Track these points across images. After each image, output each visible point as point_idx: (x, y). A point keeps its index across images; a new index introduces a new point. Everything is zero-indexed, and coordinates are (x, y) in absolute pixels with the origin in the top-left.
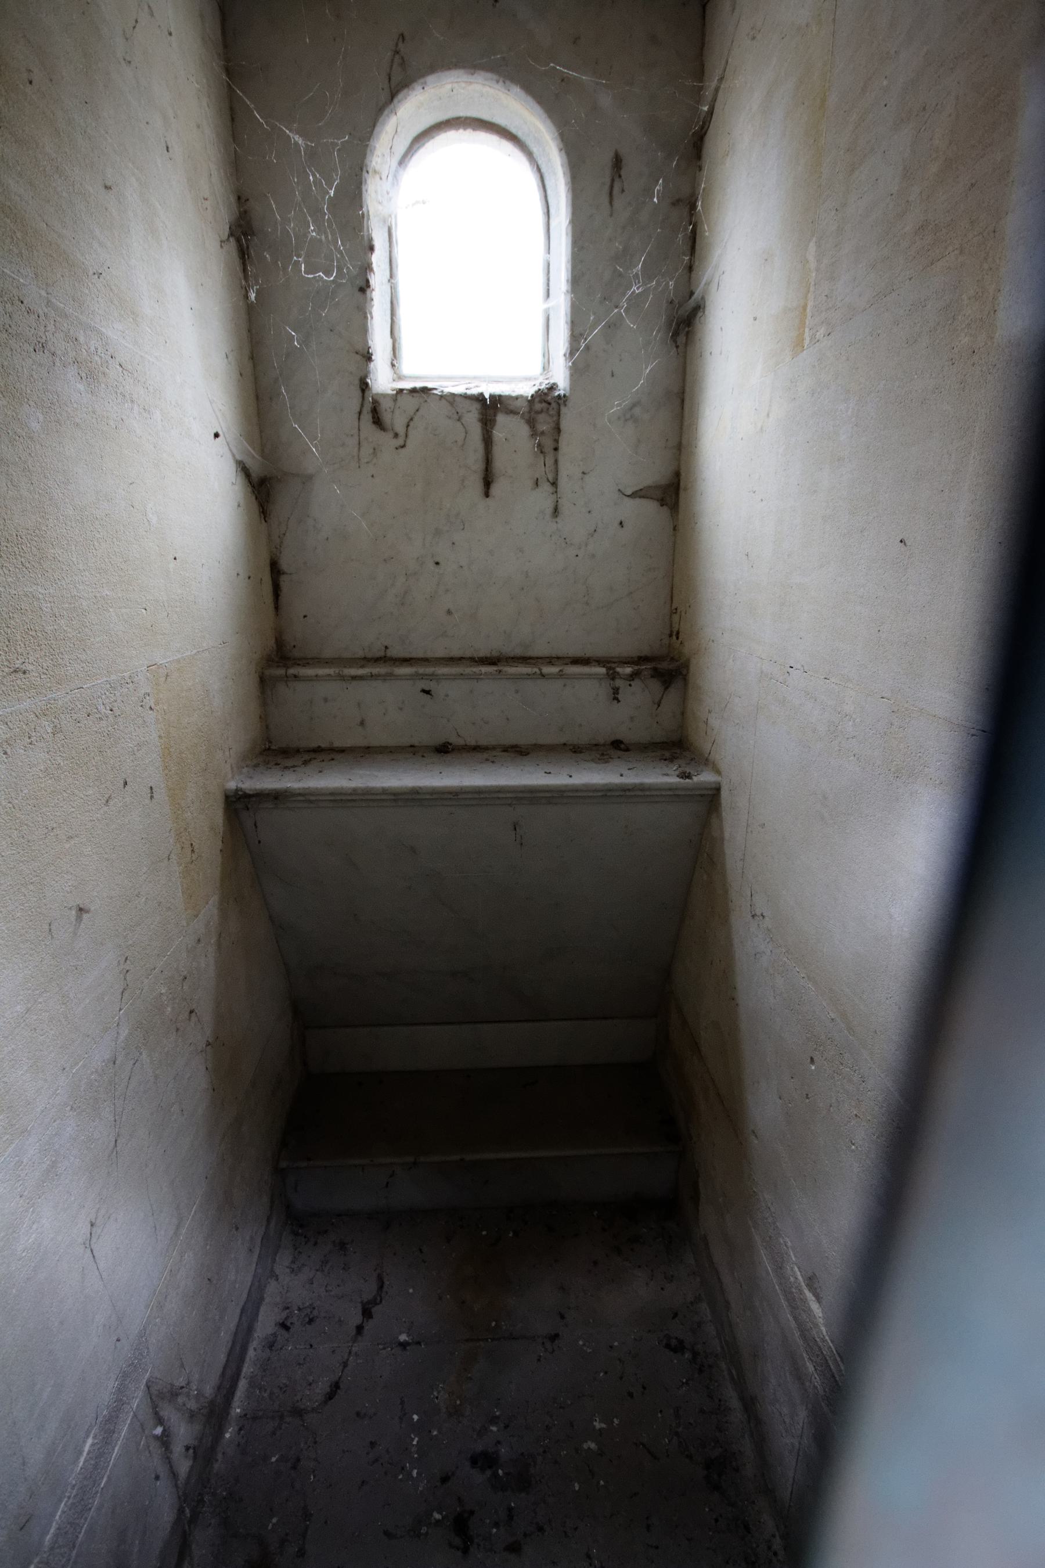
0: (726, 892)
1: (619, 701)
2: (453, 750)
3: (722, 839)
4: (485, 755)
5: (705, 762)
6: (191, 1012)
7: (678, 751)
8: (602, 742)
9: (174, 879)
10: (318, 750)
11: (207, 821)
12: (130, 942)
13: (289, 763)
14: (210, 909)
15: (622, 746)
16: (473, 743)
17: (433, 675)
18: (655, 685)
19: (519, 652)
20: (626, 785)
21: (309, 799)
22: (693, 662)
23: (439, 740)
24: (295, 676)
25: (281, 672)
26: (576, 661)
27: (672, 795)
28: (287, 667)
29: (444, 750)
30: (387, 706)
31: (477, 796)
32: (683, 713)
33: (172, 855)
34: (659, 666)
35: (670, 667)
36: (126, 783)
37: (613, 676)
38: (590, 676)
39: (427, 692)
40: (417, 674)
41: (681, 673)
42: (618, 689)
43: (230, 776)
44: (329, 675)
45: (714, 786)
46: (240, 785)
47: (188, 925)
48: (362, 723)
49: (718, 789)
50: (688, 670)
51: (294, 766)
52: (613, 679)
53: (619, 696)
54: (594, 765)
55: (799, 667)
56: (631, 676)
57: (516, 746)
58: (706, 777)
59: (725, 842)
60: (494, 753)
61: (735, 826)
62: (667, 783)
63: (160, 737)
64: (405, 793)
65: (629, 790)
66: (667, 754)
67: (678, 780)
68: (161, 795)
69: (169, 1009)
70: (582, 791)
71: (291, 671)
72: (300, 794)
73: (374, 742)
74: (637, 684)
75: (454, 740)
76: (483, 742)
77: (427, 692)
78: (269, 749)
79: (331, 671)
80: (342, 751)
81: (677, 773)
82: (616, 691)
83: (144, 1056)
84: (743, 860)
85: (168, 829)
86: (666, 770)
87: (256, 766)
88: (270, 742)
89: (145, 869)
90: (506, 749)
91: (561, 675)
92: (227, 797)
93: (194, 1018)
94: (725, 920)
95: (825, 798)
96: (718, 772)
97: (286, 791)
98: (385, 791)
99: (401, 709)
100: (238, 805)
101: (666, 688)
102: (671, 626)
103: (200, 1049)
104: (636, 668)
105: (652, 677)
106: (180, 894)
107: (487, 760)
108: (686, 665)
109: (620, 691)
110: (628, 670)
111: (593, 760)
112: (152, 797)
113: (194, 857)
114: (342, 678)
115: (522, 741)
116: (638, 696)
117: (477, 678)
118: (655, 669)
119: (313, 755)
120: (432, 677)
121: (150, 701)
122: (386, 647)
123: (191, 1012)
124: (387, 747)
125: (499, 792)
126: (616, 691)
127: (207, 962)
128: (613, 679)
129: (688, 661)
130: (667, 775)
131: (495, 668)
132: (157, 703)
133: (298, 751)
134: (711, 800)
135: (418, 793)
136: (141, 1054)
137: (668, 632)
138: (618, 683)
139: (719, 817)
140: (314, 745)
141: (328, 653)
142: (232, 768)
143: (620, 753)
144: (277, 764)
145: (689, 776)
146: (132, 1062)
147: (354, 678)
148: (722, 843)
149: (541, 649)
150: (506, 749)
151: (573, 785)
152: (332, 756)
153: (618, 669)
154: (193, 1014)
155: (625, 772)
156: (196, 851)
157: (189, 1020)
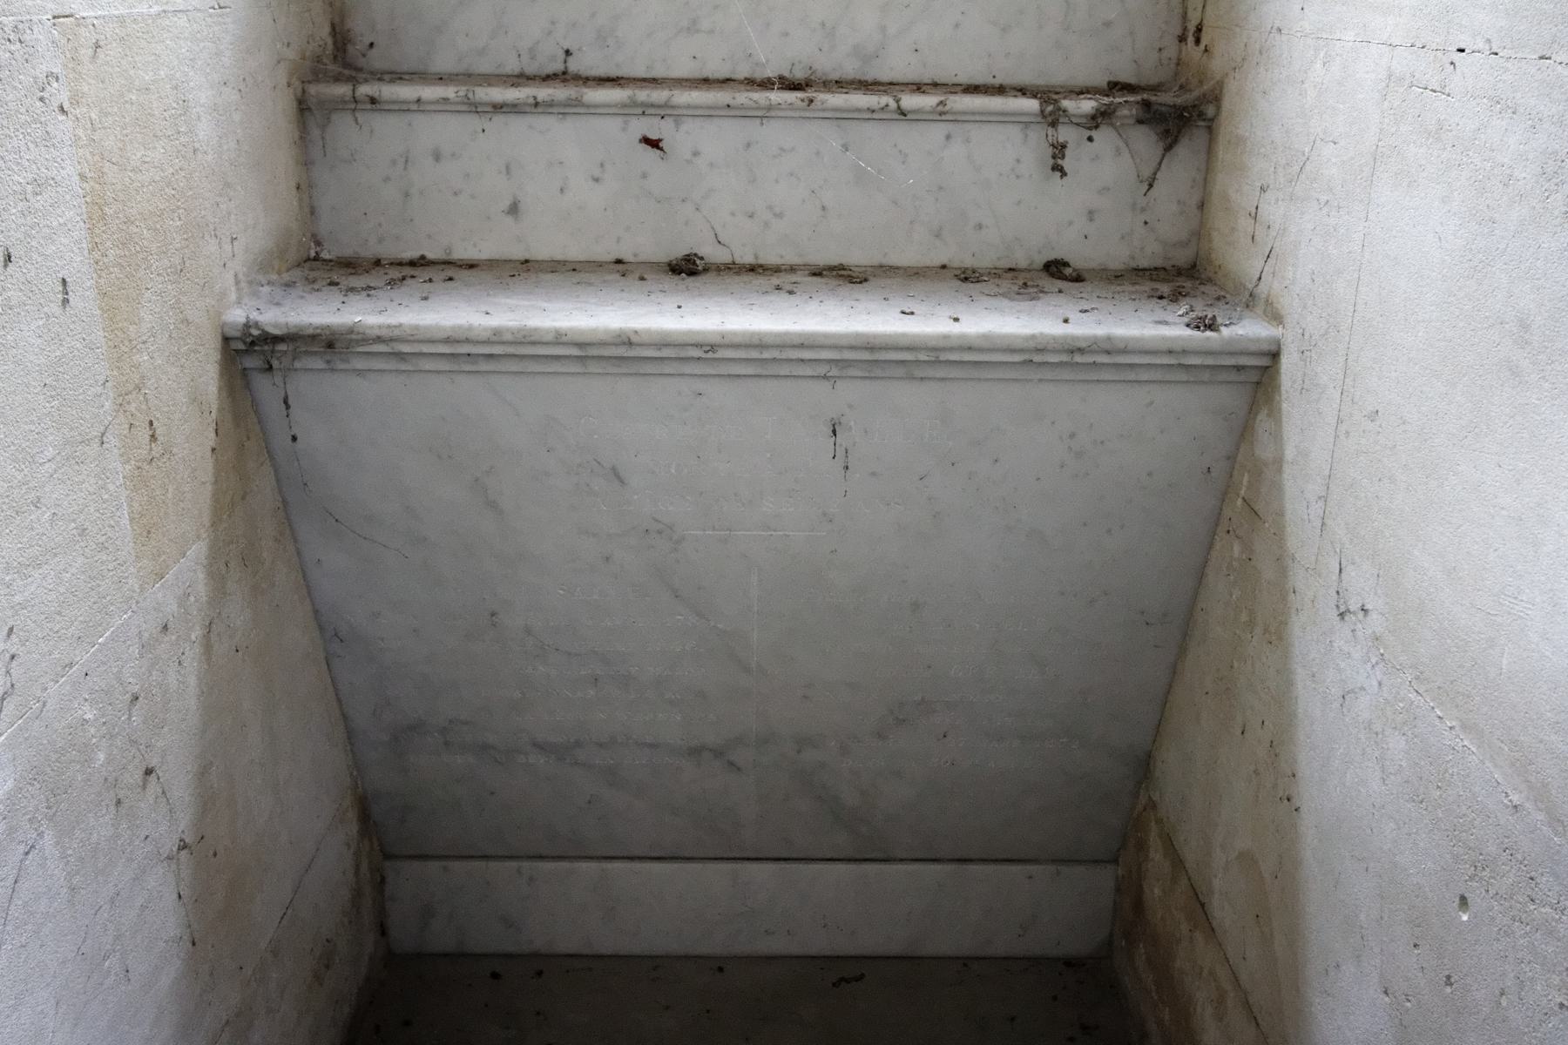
0: (1283, 571)
1: (1064, 174)
2: (706, 270)
3: (1279, 462)
4: (775, 281)
5: (1250, 300)
6: (149, 772)
7: (1188, 284)
8: (1023, 264)
9: (111, 487)
10: (421, 263)
11: (188, 384)
12: (18, 598)
13: (356, 282)
14: (190, 566)
15: (1068, 271)
16: (749, 259)
17: (666, 105)
18: (1145, 141)
19: (850, 69)
20: (1075, 338)
21: (397, 351)
22: (1231, 87)
23: (679, 251)
24: (373, 101)
25: (342, 90)
26: (973, 89)
27: (1174, 365)
28: (354, 81)
29: (686, 268)
30: (566, 173)
31: (754, 354)
32: (1202, 206)
33: (109, 437)
34: (1153, 98)
35: (1179, 101)
36: (8, 258)
37: (1053, 118)
38: (1004, 118)
39: (654, 144)
40: (633, 104)
41: (1201, 115)
42: (1064, 146)
43: (233, 297)
44: (446, 100)
45: (1265, 347)
46: (255, 316)
47: (142, 589)
48: (514, 209)
49: (1275, 355)
50: (1219, 108)
51: (369, 288)
52: (1054, 124)
53: (1066, 164)
54: (1006, 302)
55: (1481, 45)
56: (1093, 117)
57: (842, 267)
58: (1248, 330)
59: (1288, 471)
60: (794, 278)
61: (1312, 436)
62: (1164, 338)
63: (83, 177)
64: (603, 344)
65: (1081, 351)
66: (1165, 289)
67: (1189, 332)
68: (84, 299)
69: (102, 756)
70: (980, 350)
71: (365, 90)
72: (379, 339)
73: (541, 252)
74: (1105, 137)
75: (710, 252)
76: (770, 258)
77: (654, 144)
78: (316, 259)
79: (449, 92)
80: (472, 266)
81: (1186, 320)
82: (1059, 149)
83: (49, 839)
84: (1324, 499)
85: (102, 379)
86: (1160, 315)
87: (289, 285)
88: (318, 243)
89: (50, 452)
90: (817, 273)
91: (941, 114)
92: (226, 340)
93: (153, 787)
94: (1277, 634)
95: (1524, 326)
96: (1276, 318)
97: (351, 330)
98: (559, 338)
99: (597, 180)
100: (250, 356)
101: (1168, 148)
102: (1184, 16)
103: (165, 852)
104: (1106, 100)
105: (1140, 122)
106: (125, 521)
107: (778, 288)
108: (1216, 97)
109: (1068, 152)
110: (1087, 105)
111: (1004, 295)
112: (65, 302)
113: (157, 449)
114: (474, 108)
115: (856, 257)
116: (1108, 162)
117: (765, 114)
118: (1146, 104)
119: (408, 271)
120: (663, 111)
121: (60, 93)
122: (568, 53)
123: (149, 772)
124: (565, 263)
125: (802, 346)
126: (1059, 149)
127: (183, 678)
128: (1054, 124)
129: (1220, 85)
130: (1166, 323)
131: (800, 94)
132: (76, 100)
133: (378, 263)
134: (1260, 376)
135: (630, 344)
136: (41, 835)
137: (1179, 32)
138: (1065, 133)
139: (1275, 414)
140: (411, 254)
141: (443, 62)
142: (237, 283)
143: (1060, 284)
144: (332, 284)
145: (1212, 326)
146: (22, 848)
147: (498, 108)
148: (1280, 470)
149: (896, 66)
150: (817, 273)
151: (963, 336)
152: (450, 273)
153: (1066, 103)
154: (153, 777)
155: (1074, 316)
156: (161, 438)
157: (144, 787)
